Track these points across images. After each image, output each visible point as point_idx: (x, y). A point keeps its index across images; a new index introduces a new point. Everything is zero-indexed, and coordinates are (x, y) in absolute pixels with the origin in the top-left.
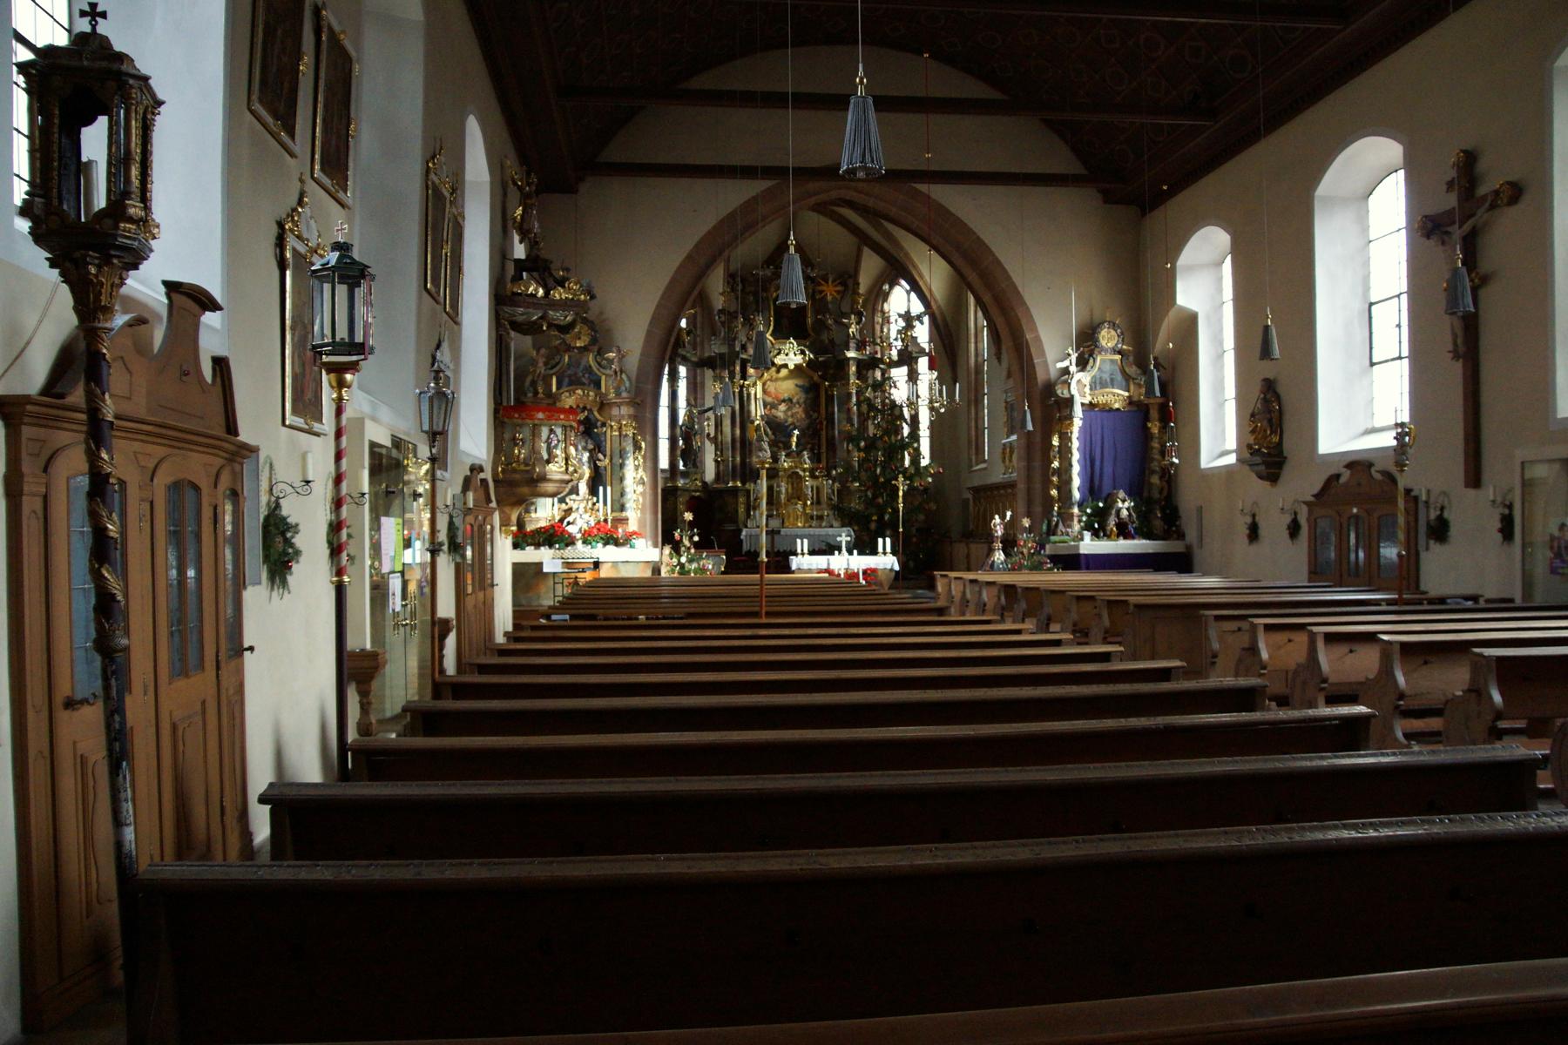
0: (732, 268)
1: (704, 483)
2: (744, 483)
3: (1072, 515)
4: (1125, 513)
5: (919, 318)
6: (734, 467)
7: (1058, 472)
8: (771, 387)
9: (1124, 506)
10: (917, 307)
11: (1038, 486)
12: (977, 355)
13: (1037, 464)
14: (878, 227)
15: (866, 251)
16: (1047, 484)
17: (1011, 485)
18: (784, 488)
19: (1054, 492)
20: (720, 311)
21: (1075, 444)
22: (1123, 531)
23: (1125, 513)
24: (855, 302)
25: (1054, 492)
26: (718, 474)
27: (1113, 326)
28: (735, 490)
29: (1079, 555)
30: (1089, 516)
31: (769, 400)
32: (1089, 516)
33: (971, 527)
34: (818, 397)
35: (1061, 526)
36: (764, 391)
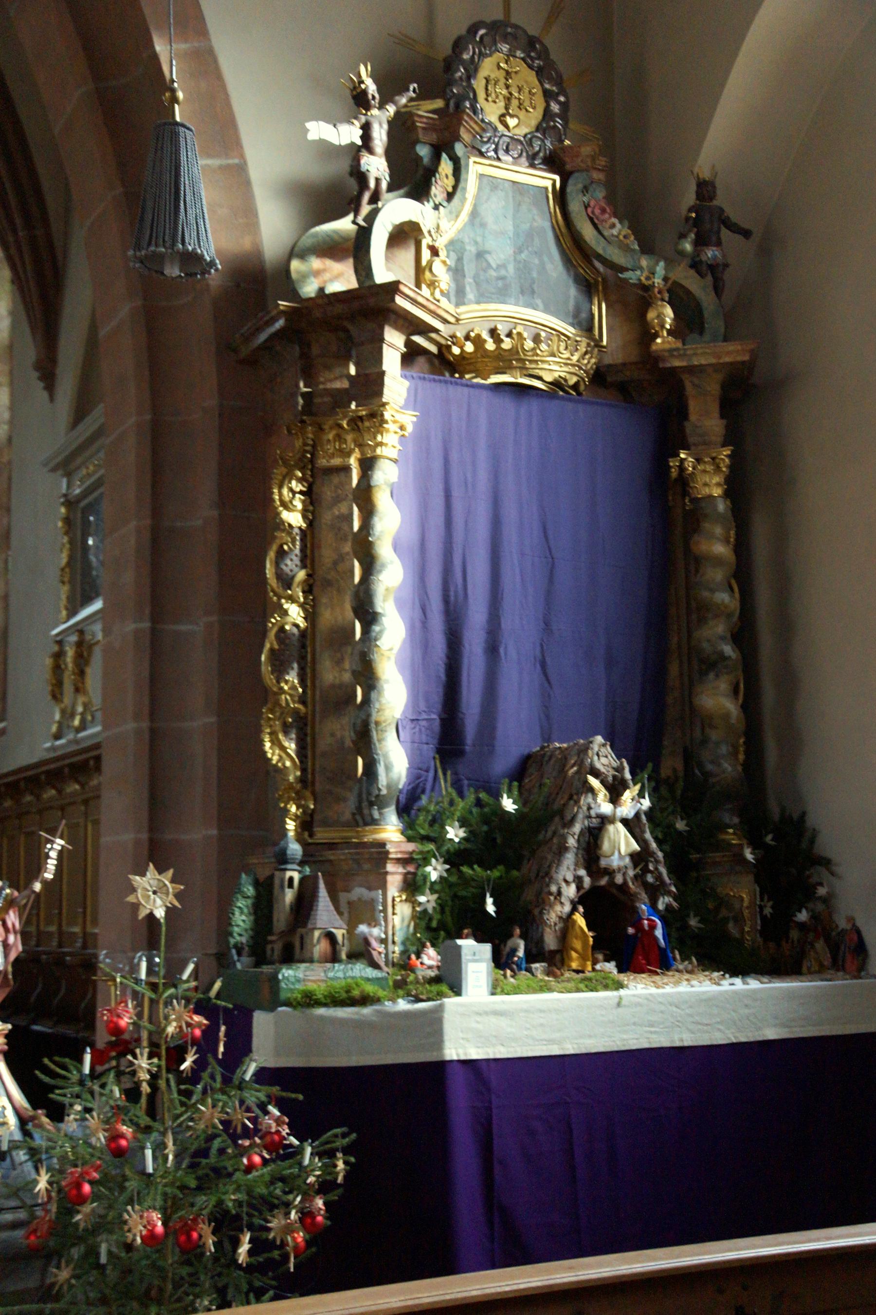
3: (379, 853)
4: (620, 844)
7: (301, 649)
9: (619, 815)
11: (198, 724)
13: (197, 627)
16: (243, 702)
17: (83, 765)
19: (281, 751)
21: (390, 522)
22: (622, 943)
23: (620, 844)
25: (281, 751)
27: (532, 48)
29: (442, 1066)
30: (455, 858)
32: (455, 858)
35: (325, 915)
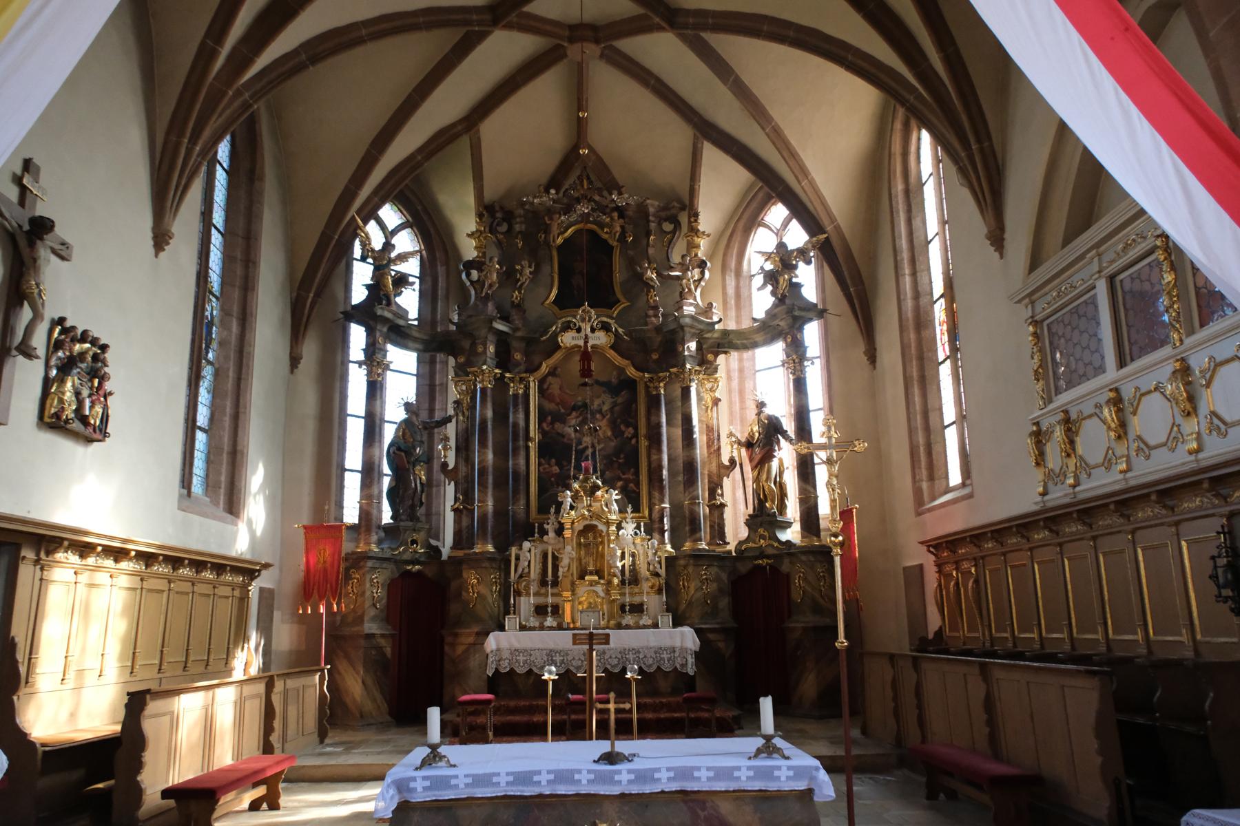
0: (488, 195)
1: (437, 551)
2: (502, 547)
5: (802, 253)
6: (483, 518)
8: (555, 385)
10: (797, 236)
12: (917, 296)
14: (721, 68)
15: (711, 155)
18: (569, 554)
20: (469, 265)
24: (692, 246)
26: (458, 534)
28: (477, 561)
31: (549, 406)
33: (934, 621)
34: (633, 399)
36: (542, 392)
